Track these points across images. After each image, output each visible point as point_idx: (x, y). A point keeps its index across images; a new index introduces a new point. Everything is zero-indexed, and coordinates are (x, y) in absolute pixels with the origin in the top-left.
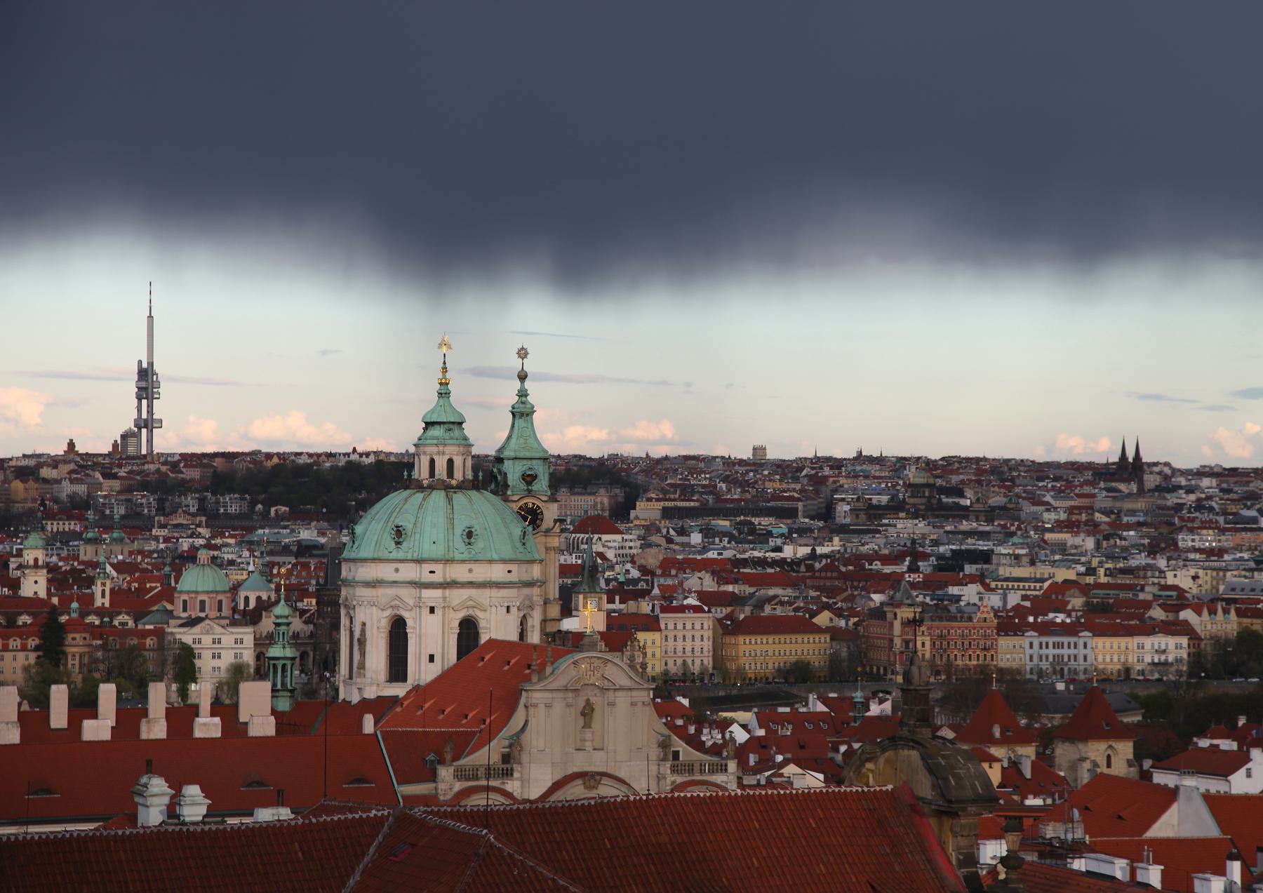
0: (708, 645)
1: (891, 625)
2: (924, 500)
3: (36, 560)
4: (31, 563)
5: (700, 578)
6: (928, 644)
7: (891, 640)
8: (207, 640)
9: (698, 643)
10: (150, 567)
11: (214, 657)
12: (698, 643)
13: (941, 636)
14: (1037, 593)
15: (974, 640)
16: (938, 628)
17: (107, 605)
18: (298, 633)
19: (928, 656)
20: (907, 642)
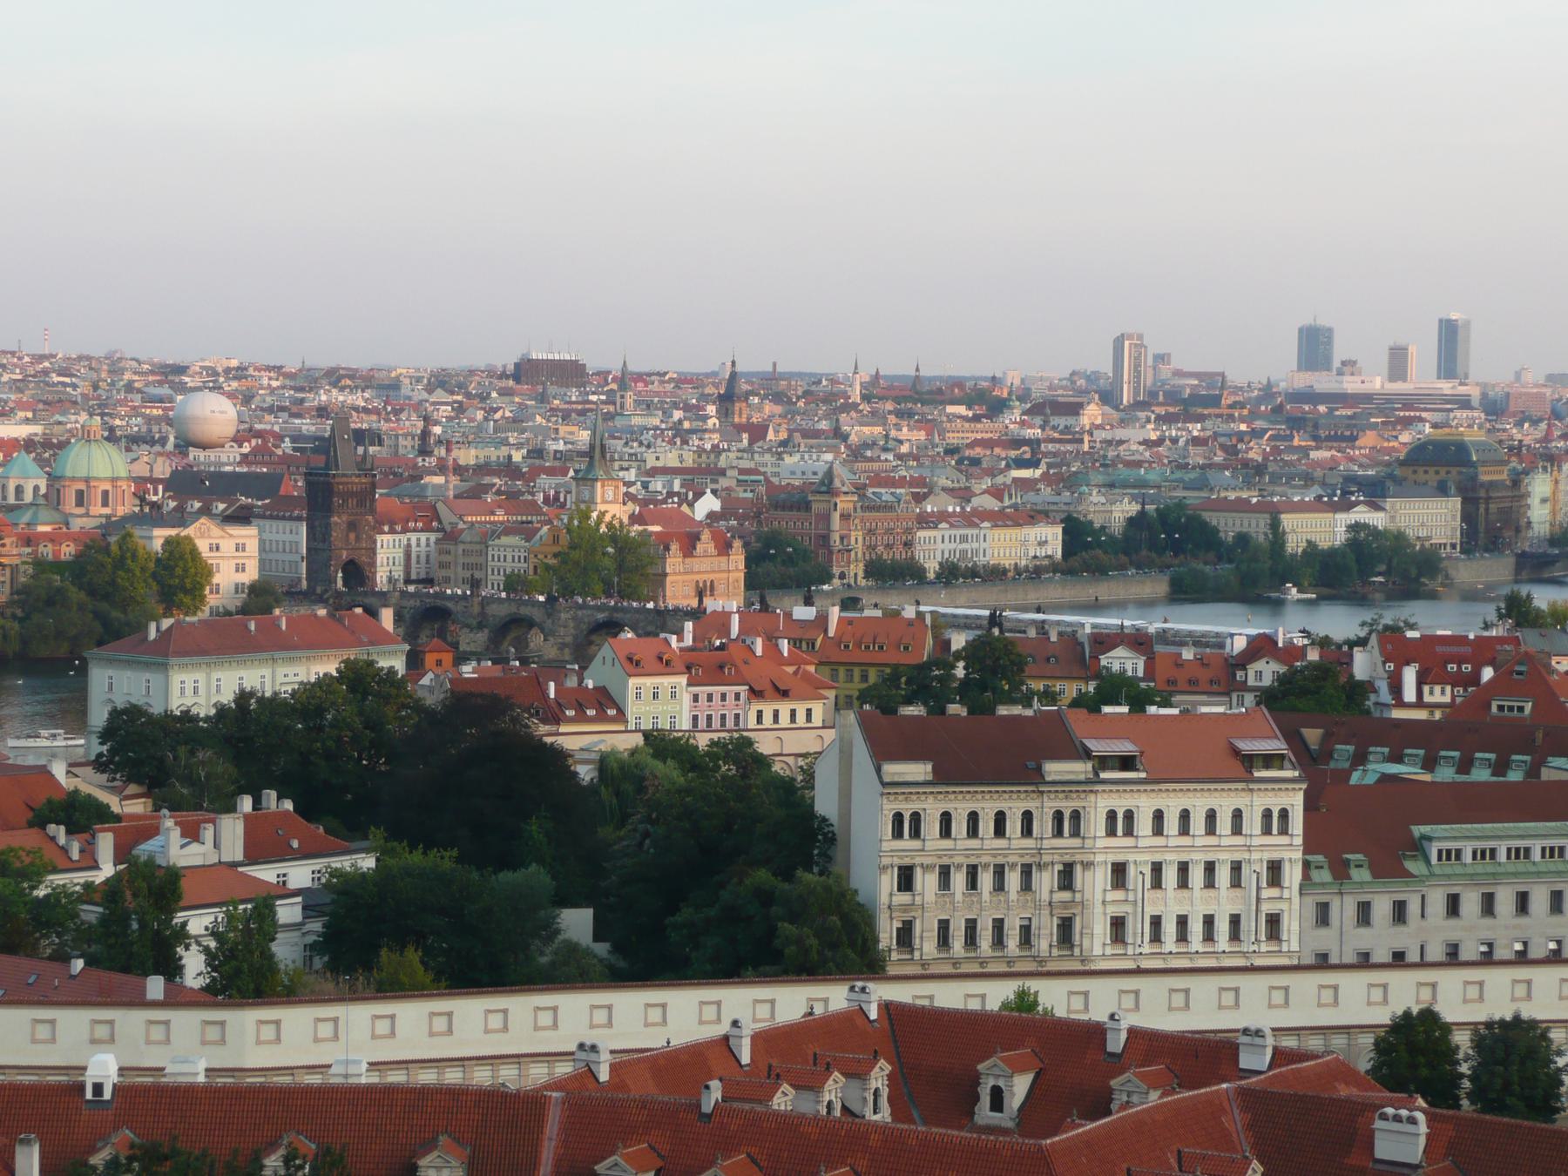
1: (826, 518)
15: (898, 533)
20: (842, 538)
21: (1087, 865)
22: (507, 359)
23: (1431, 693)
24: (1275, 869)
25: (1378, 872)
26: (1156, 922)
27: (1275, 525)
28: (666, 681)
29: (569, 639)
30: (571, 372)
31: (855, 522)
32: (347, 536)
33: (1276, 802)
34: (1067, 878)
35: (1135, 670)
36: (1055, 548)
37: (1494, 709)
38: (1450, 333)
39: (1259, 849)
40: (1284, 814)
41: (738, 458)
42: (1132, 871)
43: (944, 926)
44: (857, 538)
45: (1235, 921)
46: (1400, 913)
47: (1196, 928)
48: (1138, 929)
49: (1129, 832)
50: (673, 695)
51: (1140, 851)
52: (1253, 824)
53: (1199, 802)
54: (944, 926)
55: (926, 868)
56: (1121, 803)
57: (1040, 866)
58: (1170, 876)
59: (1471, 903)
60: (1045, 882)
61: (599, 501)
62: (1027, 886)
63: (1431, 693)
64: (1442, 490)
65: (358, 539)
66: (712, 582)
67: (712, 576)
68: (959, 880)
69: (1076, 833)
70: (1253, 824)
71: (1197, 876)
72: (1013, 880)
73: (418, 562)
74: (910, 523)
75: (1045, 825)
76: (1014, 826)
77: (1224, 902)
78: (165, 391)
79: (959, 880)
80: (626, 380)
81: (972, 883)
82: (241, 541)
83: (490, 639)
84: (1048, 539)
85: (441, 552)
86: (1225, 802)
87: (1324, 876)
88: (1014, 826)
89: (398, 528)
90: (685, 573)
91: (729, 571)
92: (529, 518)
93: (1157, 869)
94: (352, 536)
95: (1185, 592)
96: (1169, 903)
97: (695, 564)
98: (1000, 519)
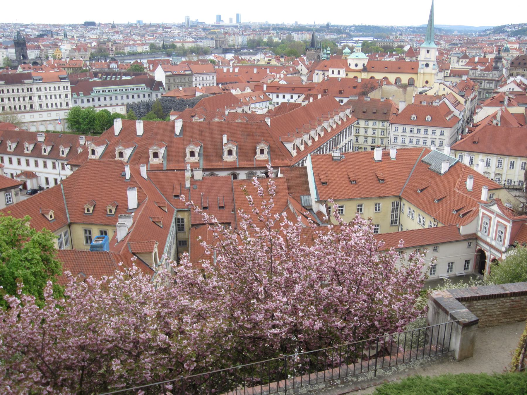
21: (34, 96)
22: (83, 23)
24: (66, 96)
25: (85, 95)
26: (47, 104)
27: (183, 45)
30: (93, 24)
33: (65, 85)
34: (31, 98)
36: (148, 49)
38: (238, 16)
39: (63, 92)
40: (67, 87)
42: (42, 97)
43: (10, 107)
44: (114, 49)
45: (61, 104)
46: (88, 101)
47: (54, 105)
48: (44, 106)
49: (41, 91)
51: (43, 93)
52: (62, 88)
53: (52, 86)
54: (10, 107)
55: (6, 98)
56: (39, 86)
57: (26, 97)
58: (49, 97)
59: (102, 99)
60: (27, 99)
62: (24, 100)
64: (212, 39)
68: (12, 100)
69: (31, 91)
70: (62, 88)
71: (53, 97)
72: (21, 99)
75: (25, 90)
76: (20, 91)
77: (58, 101)
78: (23, 29)
79: (12, 100)
80: (100, 24)
81: (19, 100)
84: (147, 48)
86: (57, 86)
87: (76, 96)
88: (20, 91)
93: (46, 96)
95: (169, 55)
96: (49, 101)
97: (81, 53)
98: (139, 45)
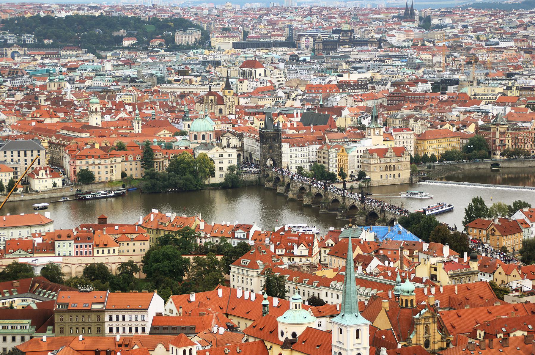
0: (413, 145)
1: (494, 133)
2: (348, 38)
3: (96, 109)
4: (94, 110)
5: (346, 99)
6: (510, 141)
7: (495, 140)
8: (217, 156)
9: (409, 144)
10: (87, 95)
11: (220, 163)
12: (409, 144)
13: (516, 137)
14: (494, 101)
15: (530, 138)
16: (515, 134)
17: (140, 132)
18: (236, 146)
19: (510, 146)
20: (501, 141)
23: (279, 251)
28: (67, 243)
29: (295, 192)
31: (508, 135)
32: (269, 151)
35: (244, 236)
37: (242, 263)
41: (465, 112)
50: (70, 246)
61: (372, 134)
63: (279, 251)
65: (273, 152)
66: (394, 165)
67: (394, 164)
73: (313, 155)
74: (527, 135)
82: (230, 153)
83: (285, 189)
85: (319, 152)
89: (295, 145)
90: (380, 163)
91: (402, 162)
92: (356, 139)
94: (271, 151)
